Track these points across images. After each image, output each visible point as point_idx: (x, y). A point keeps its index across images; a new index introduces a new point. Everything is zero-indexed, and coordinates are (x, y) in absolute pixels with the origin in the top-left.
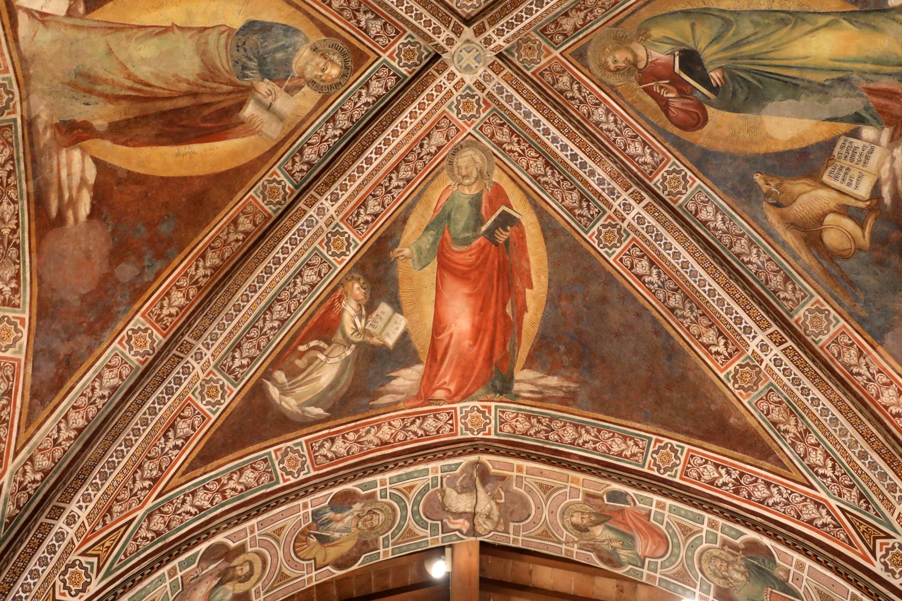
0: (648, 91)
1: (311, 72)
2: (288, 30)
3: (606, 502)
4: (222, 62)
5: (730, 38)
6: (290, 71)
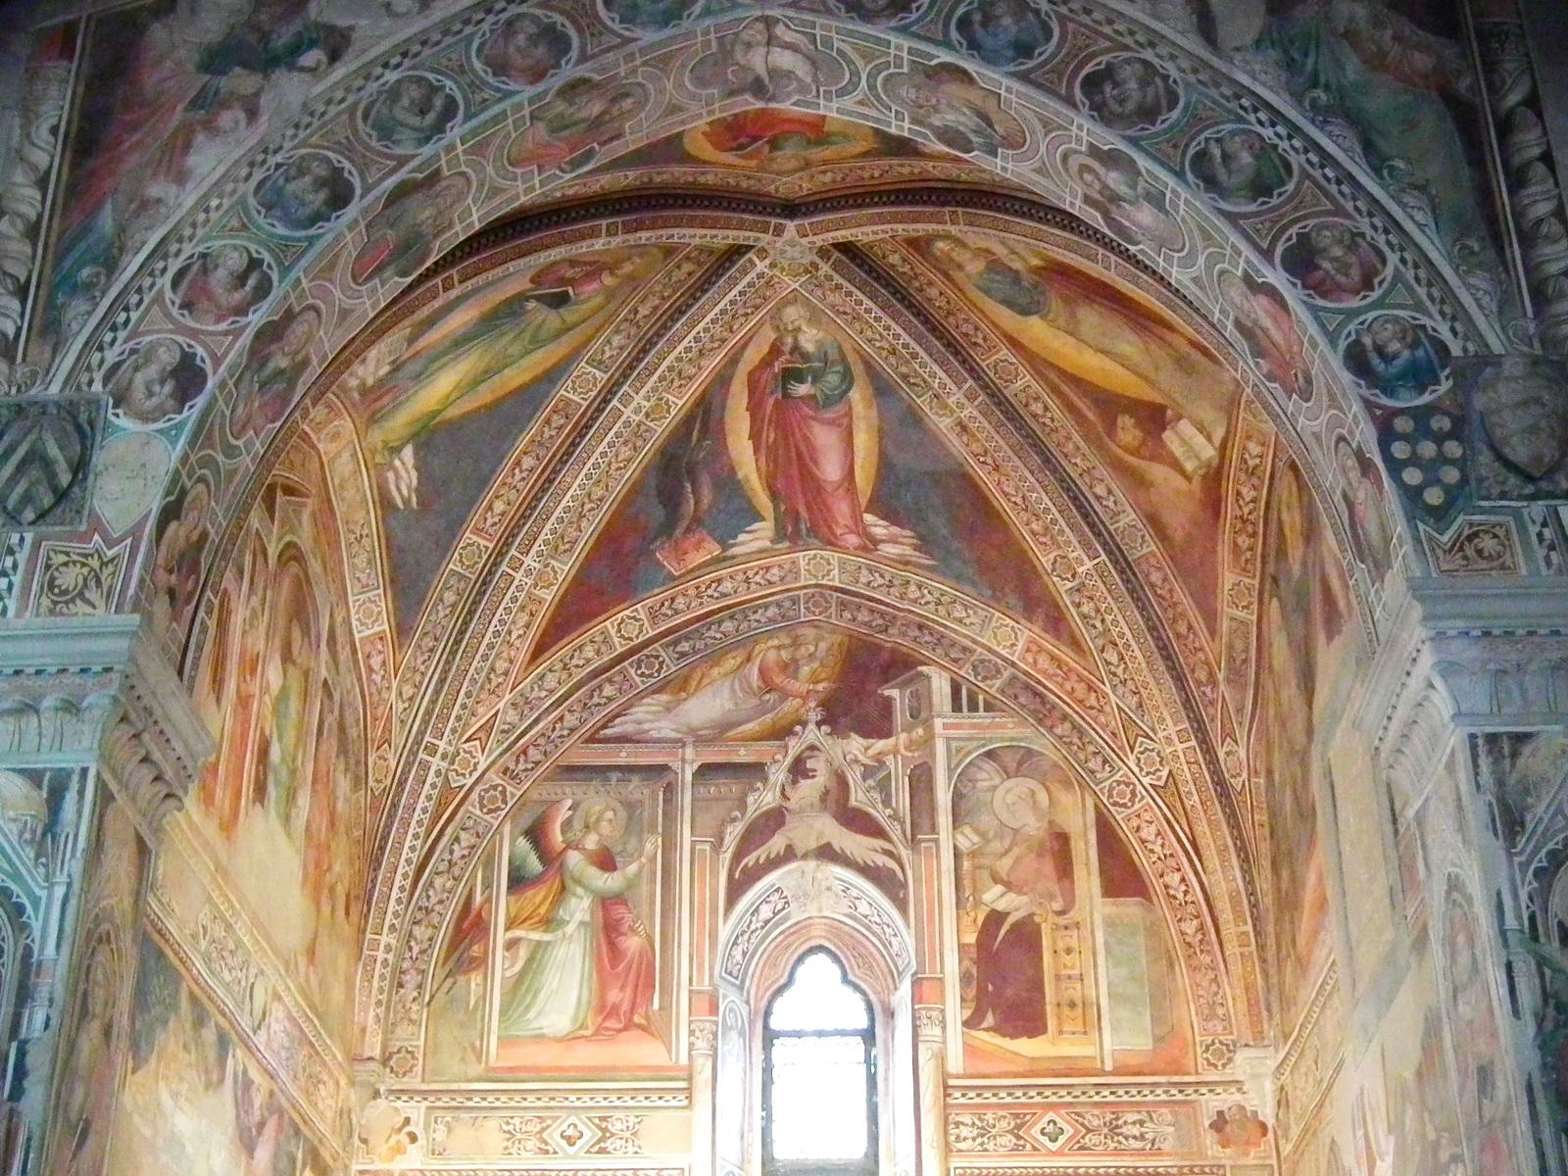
0: (595, 262)
1: (968, 255)
2: (987, 292)
3: (595, 145)
4: (1056, 305)
5: (527, 335)
6: (988, 263)
